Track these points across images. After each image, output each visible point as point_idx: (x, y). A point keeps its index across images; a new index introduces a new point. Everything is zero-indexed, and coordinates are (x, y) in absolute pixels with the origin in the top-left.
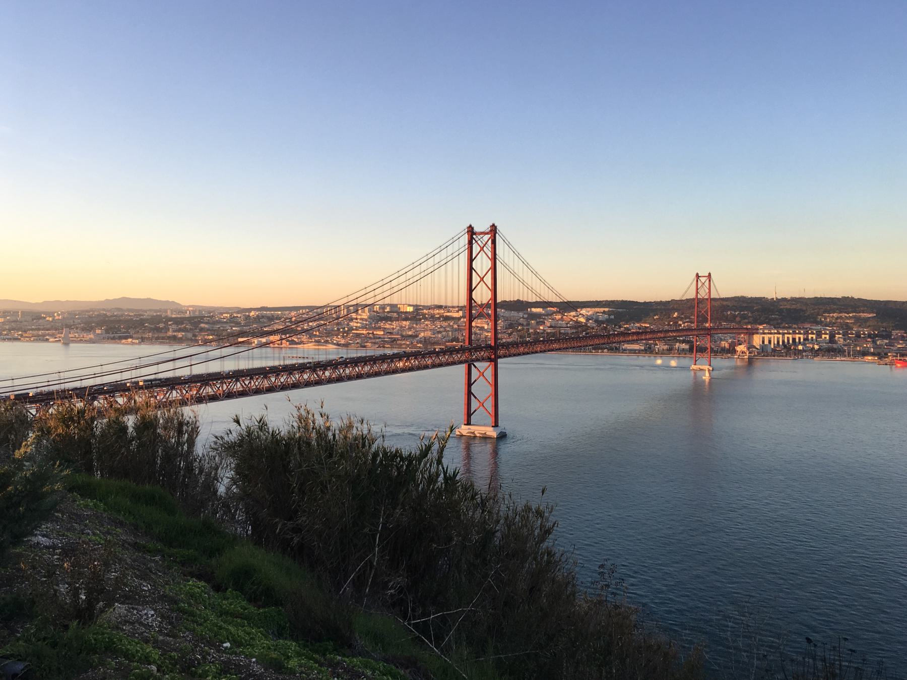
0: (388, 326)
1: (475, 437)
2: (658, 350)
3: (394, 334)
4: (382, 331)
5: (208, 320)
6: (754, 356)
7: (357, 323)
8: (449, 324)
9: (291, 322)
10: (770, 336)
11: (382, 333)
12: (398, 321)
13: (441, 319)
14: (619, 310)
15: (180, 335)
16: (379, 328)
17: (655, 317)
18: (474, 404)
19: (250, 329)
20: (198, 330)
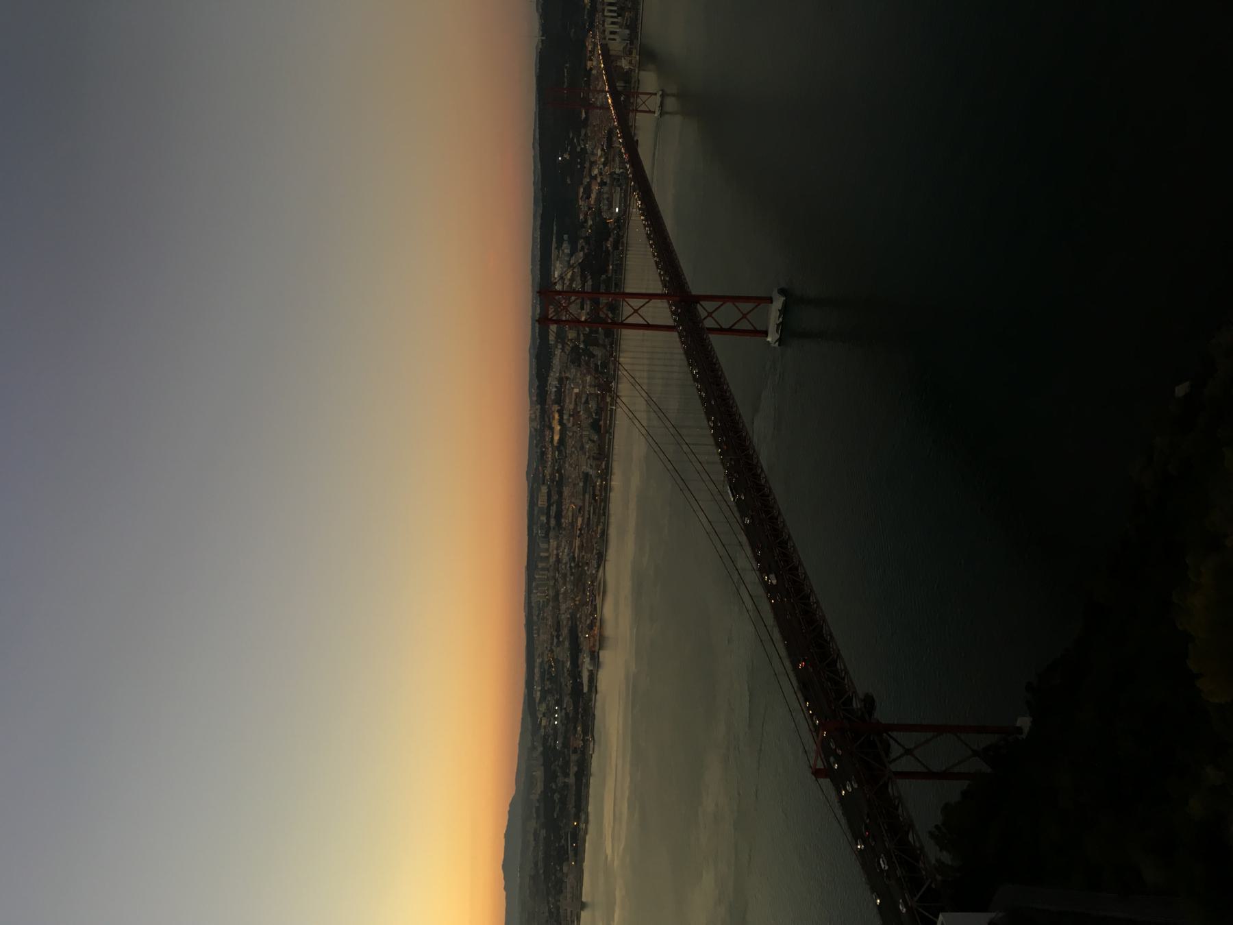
0: (570, 514)
1: (781, 323)
2: (622, 168)
3: (581, 504)
4: (578, 517)
5: (551, 739)
6: (636, 49)
7: (563, 552)
8: (571, 437)
9: (558, 637)
10: (606, 33)
11: (580, 520)
12: (562, 502)
13: (562, 448)
14: (555, 228)
15: (574, 769)
16: (573, 524)
17: (569, 181)
18: (744, 325)
19: (566, 685)
20: (566, 750)
